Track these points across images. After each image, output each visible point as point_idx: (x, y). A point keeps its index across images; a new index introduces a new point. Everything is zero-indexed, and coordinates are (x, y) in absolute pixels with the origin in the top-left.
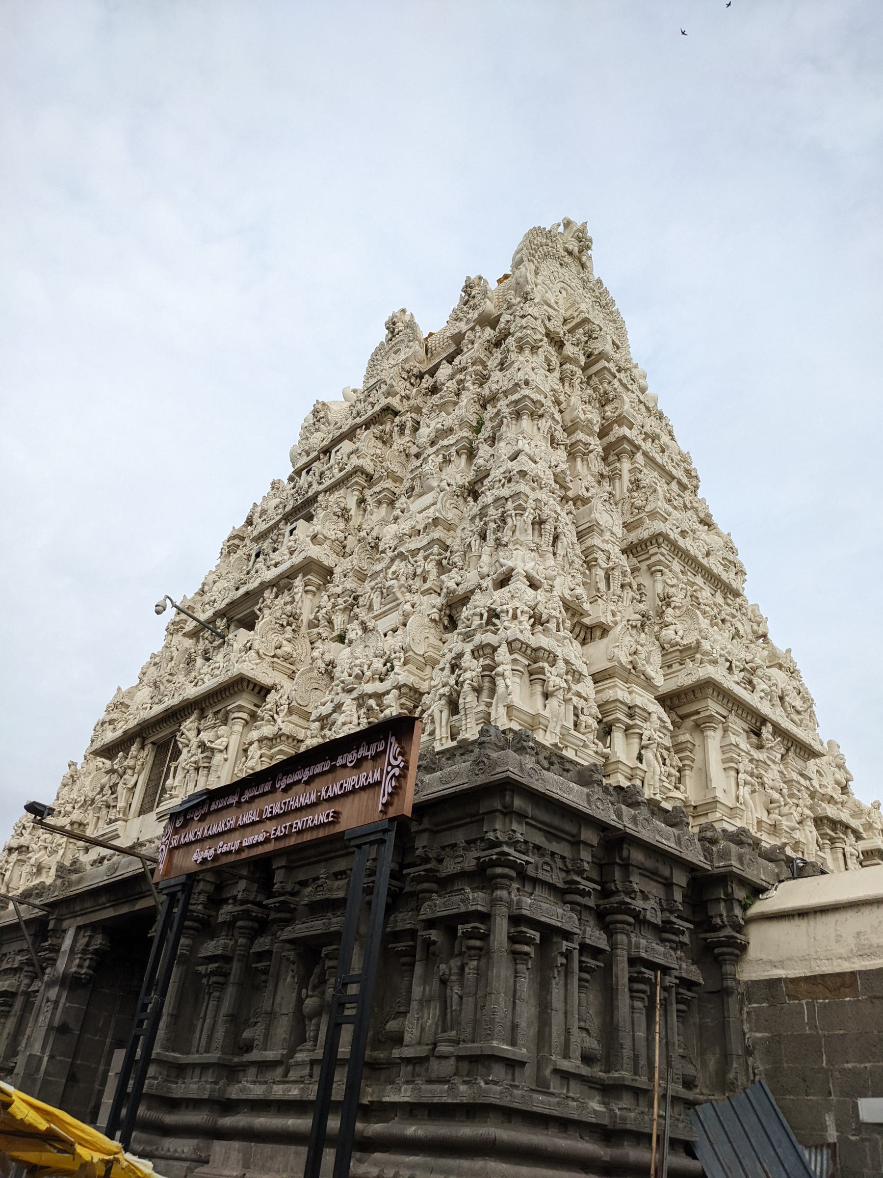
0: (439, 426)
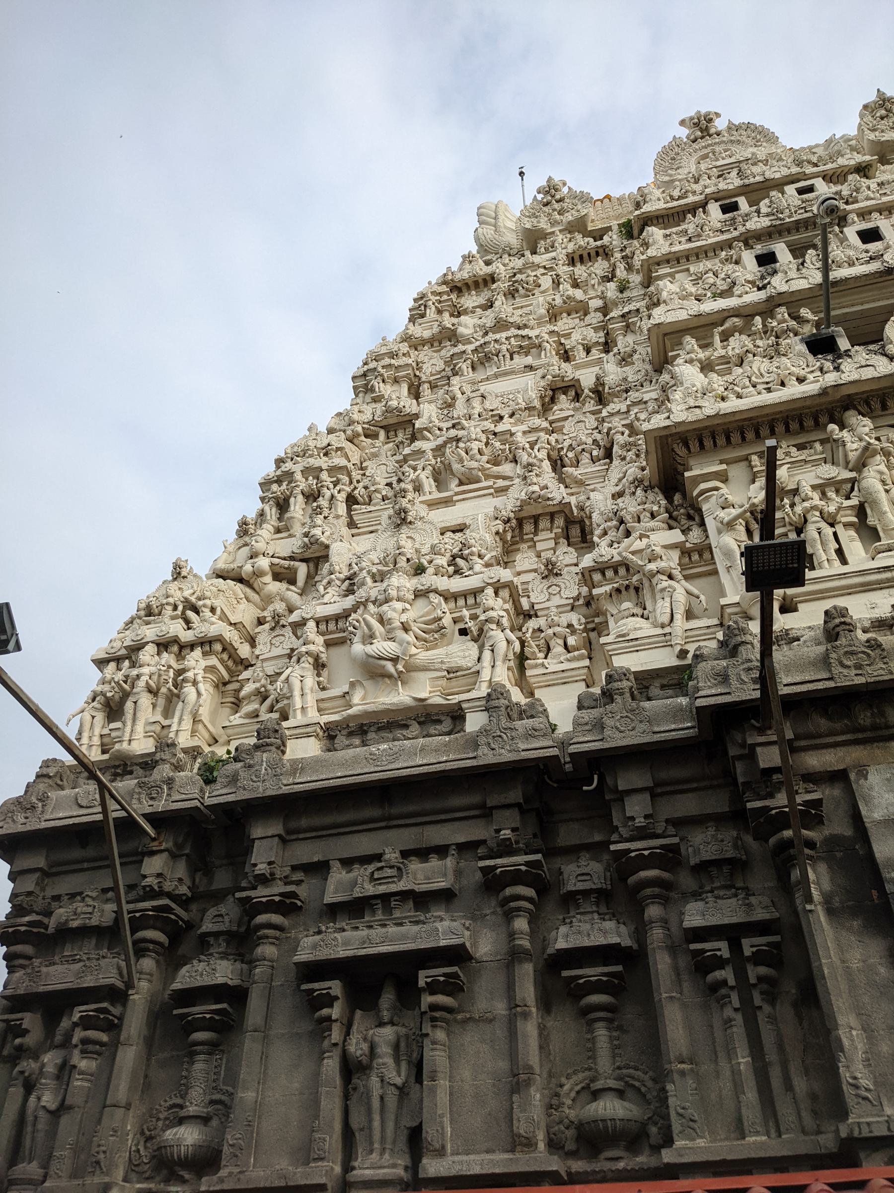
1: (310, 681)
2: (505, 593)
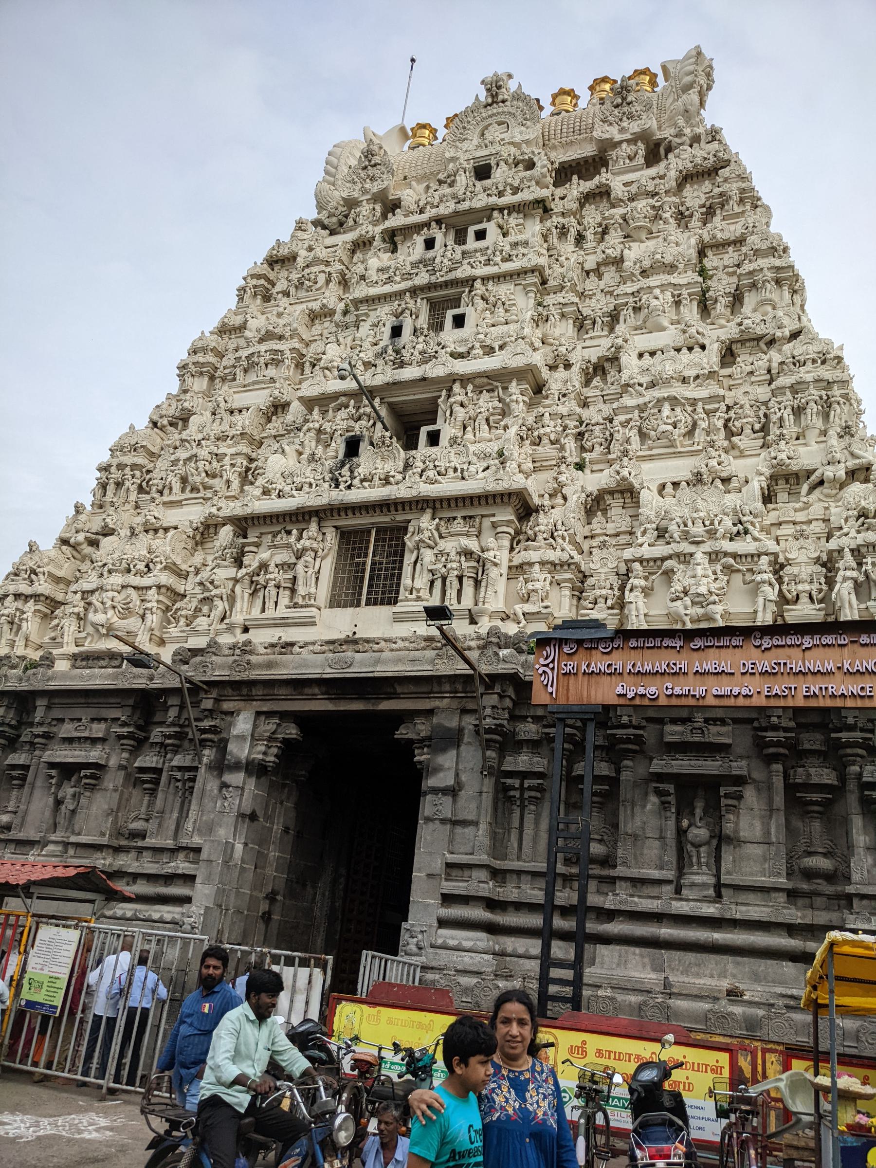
0: (658, 256)
1: (74, 627)
2: (163, 590)
